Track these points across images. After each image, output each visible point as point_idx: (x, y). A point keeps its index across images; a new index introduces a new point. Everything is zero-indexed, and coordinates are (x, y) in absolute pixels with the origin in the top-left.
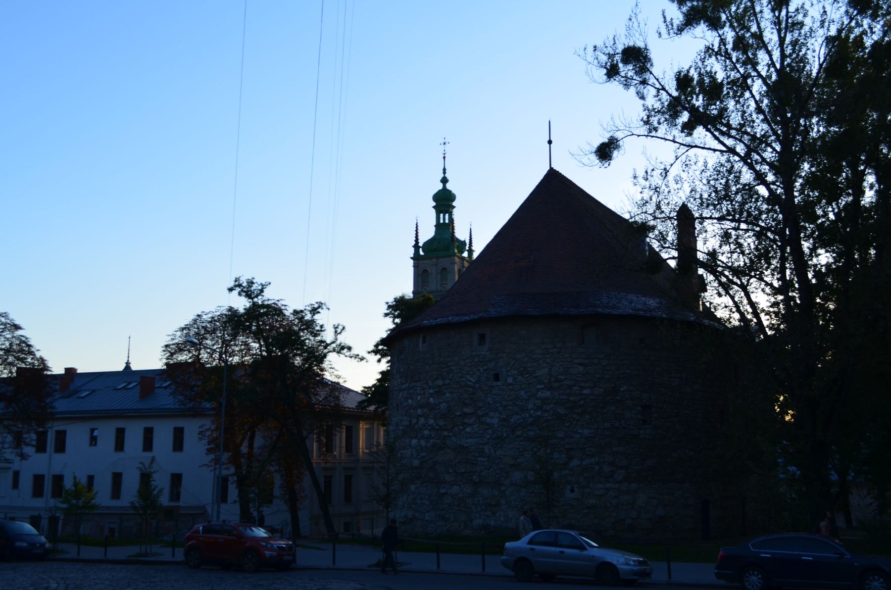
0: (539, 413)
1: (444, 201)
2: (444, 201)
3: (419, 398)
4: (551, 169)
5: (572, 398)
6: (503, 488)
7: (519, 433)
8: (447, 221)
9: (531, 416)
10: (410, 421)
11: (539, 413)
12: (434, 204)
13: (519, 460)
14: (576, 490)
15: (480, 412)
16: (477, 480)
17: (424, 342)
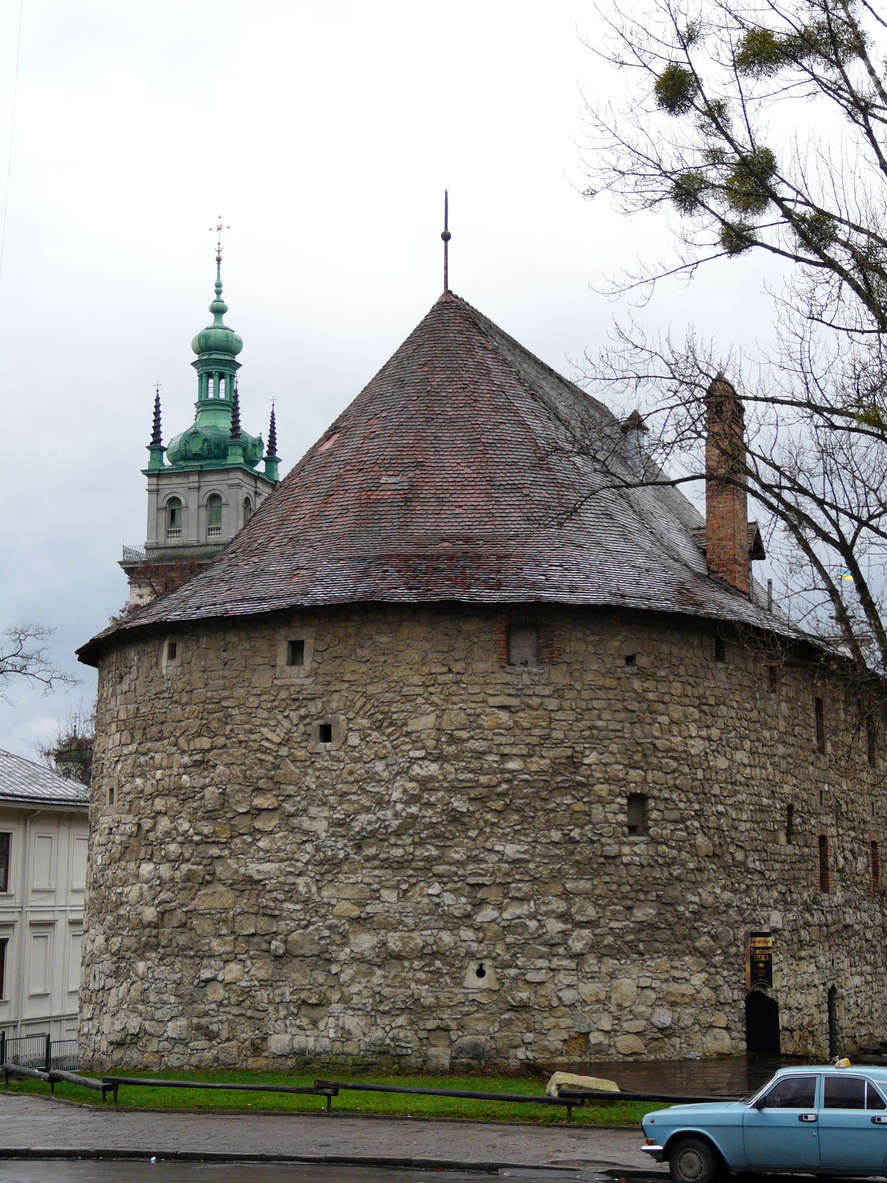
0: (414, 809)
1: (217, 357)
2: (217, 357)
3: (159, 774)
4: (448, 292)
5: (483, 779)
6: (334, 969)
7: (371, 851)
8: (222, 396)
9: (396, 815)
10: (139, 826)
11: (414, 809)
12: (196, 357)
13: (369, 909)
14: (488, 971)
15: (289, 807)
16: (281, 951)
17: (172, 655)
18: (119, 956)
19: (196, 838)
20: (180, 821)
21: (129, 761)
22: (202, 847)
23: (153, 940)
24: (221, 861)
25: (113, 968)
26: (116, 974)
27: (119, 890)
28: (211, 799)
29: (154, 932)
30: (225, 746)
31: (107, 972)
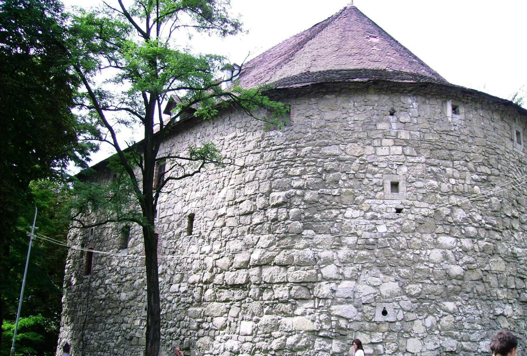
18: (419, 298)
19: (486, 225)
20: (474, 213)
21: (418, 167)
22: (492, 232)
23: (458, 288)
24: (499, 242)
25: (416, 305)
26: (418, 311)
27: (418, 252)
28: (495, 204)
29: (460, 282)
30: (499, 175)
31: (409, 308)
